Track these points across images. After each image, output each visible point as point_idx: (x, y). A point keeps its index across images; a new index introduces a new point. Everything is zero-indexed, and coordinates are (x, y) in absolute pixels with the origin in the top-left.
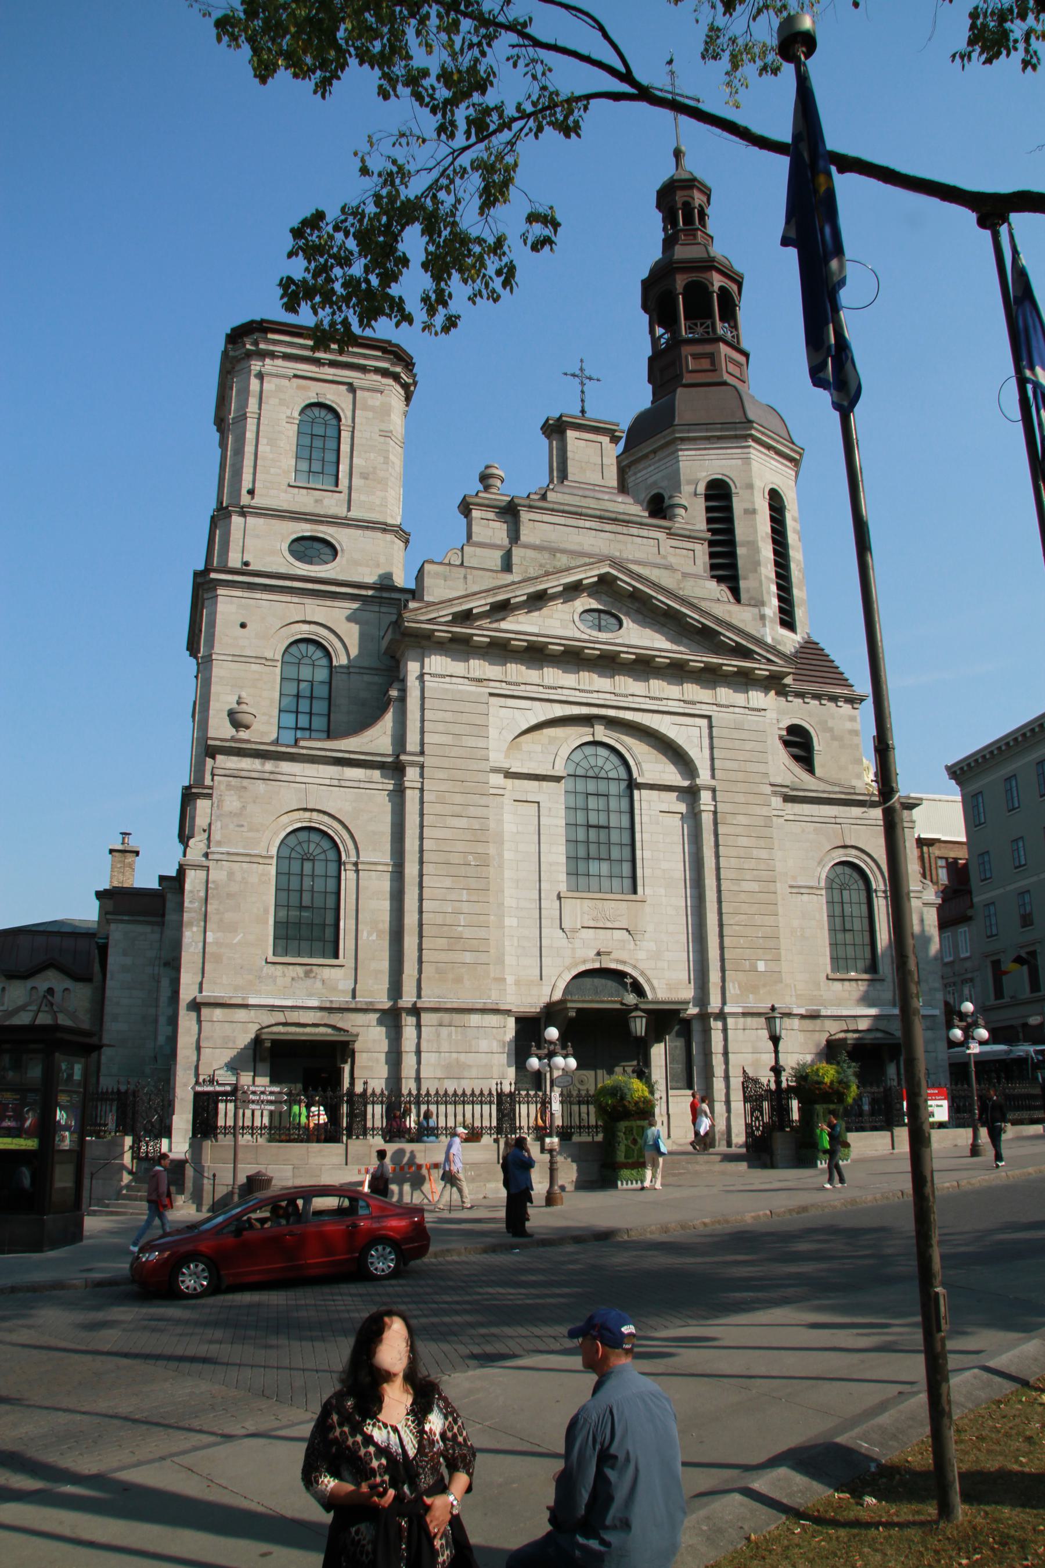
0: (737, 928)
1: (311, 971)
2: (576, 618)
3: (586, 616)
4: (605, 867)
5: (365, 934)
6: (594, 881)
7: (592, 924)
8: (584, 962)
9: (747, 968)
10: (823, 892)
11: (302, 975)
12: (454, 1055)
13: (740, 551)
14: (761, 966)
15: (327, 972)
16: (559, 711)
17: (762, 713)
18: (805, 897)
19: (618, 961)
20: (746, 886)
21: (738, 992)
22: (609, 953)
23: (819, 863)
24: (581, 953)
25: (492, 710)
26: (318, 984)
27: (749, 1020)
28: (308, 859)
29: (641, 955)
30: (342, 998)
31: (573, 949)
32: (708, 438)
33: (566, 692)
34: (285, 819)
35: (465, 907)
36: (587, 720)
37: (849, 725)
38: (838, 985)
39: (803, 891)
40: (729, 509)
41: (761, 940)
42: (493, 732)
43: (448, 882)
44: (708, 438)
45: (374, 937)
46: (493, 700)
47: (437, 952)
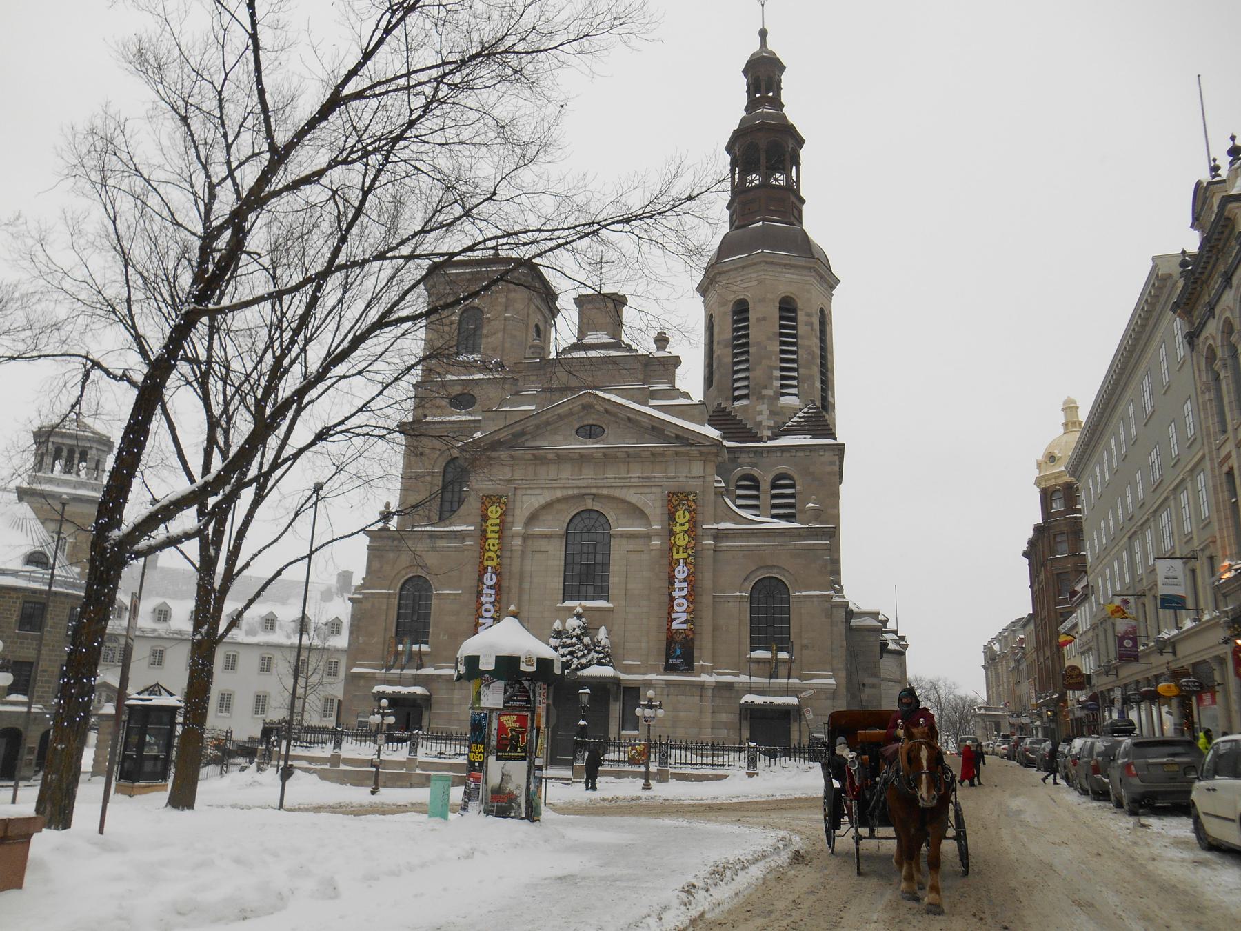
2: (574, 432)
3: (582, 430)
13: (752, 350)
16: (559, 494)
17: (701, 479)
18: (731, 604)
23: (745, 580)
25: (518, 498)
27: (672, 689)
32: (735, 269)
33: (562, 481)
34: (403, 572)
36: (584, 495)
37: (828, 469)
38: (754, 666)
40: (747, 319)
42: (517, 512)
44: (735, 269)
45: (446, 637)
46: (519, 492)
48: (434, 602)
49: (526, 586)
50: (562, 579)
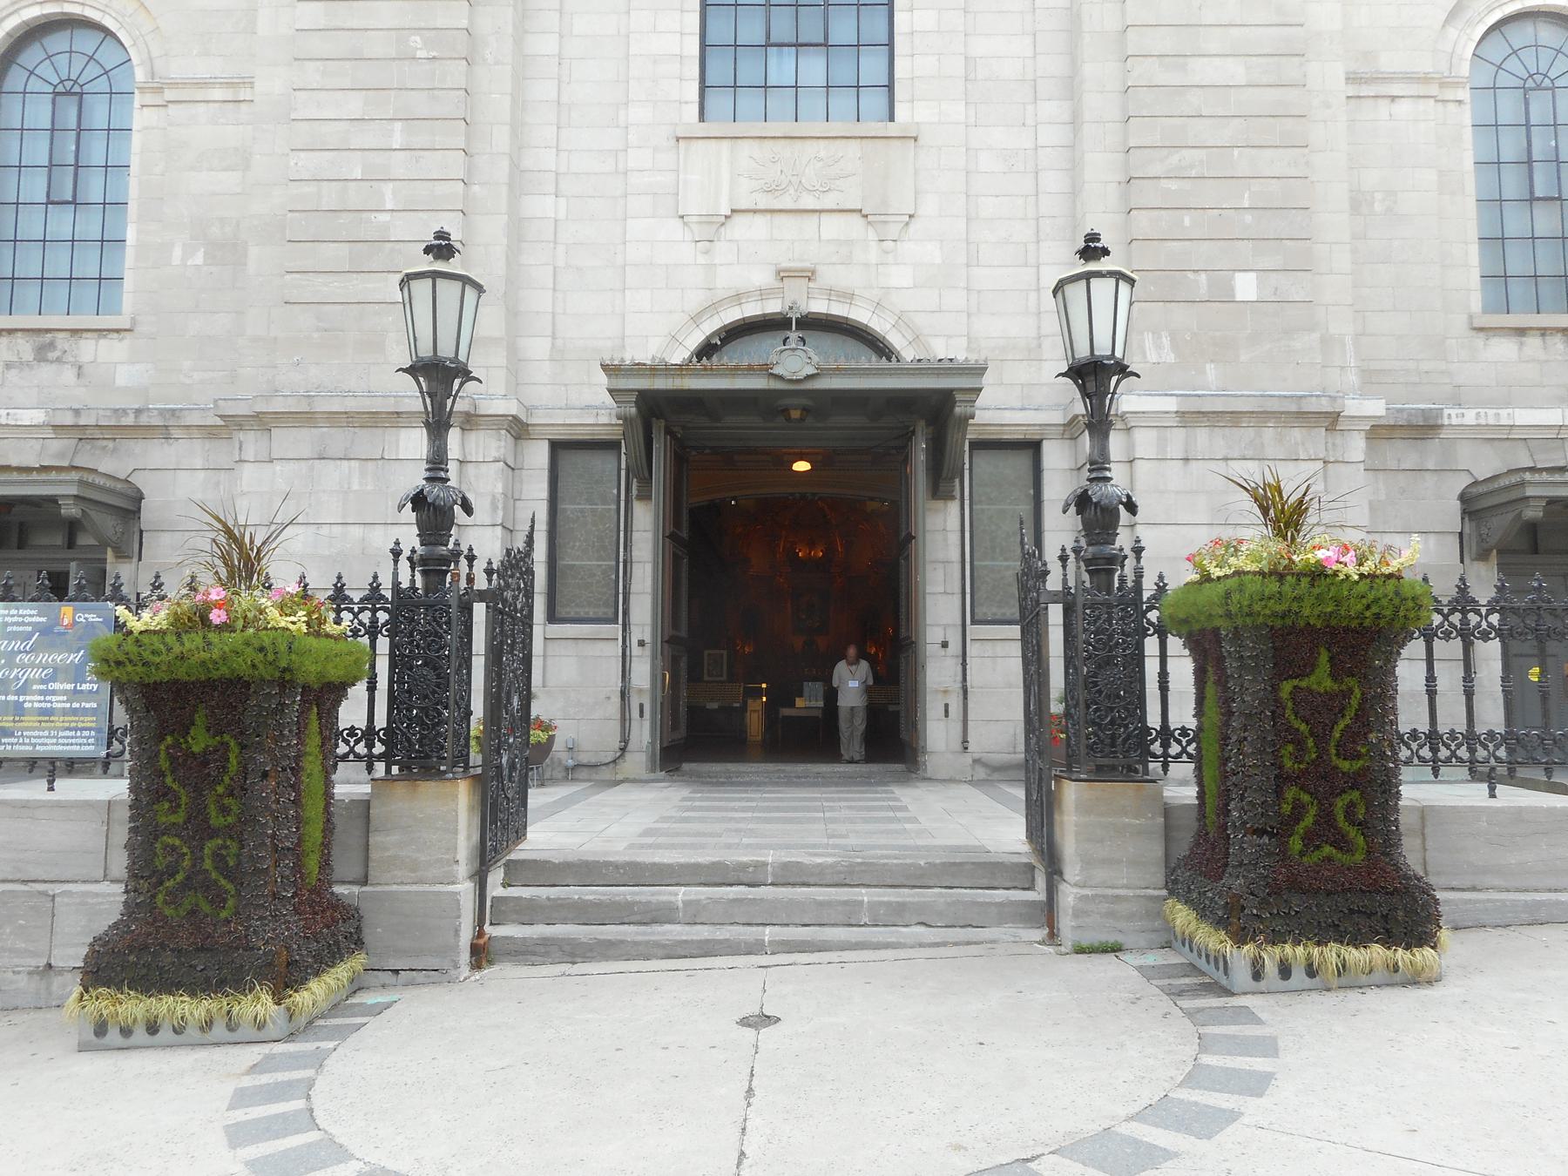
0: (1173, 185)
1: (52, 345)
4: (813, 68)
5: (177, 252)
6: (780, 102)
7: (764, 202)
8: (738, 298)
9: (1203, 292)
10: (1464, 94)
11: (28, 355)
12: (356, 531)
14: (1246, 287)
15: (87, 349)
18: (1403, 108)
19: (831, 293)
20: (1205, 71)
21: (1171, 358)
22: (810, 275)
24: (730, 278)
26: (69, 375)
28: (68, 93)
29: (900, 277)
30: (98, 406)
31: (710, 267)
35: (399, 165)
38: (1504, 349)
39: (1395, 89)
41: (1248, 218)
43: (354, 105)
45: (199, 259)
47: (321, 279)
48: (141, 119)
49: (546, 45)
50: (694, 20)
